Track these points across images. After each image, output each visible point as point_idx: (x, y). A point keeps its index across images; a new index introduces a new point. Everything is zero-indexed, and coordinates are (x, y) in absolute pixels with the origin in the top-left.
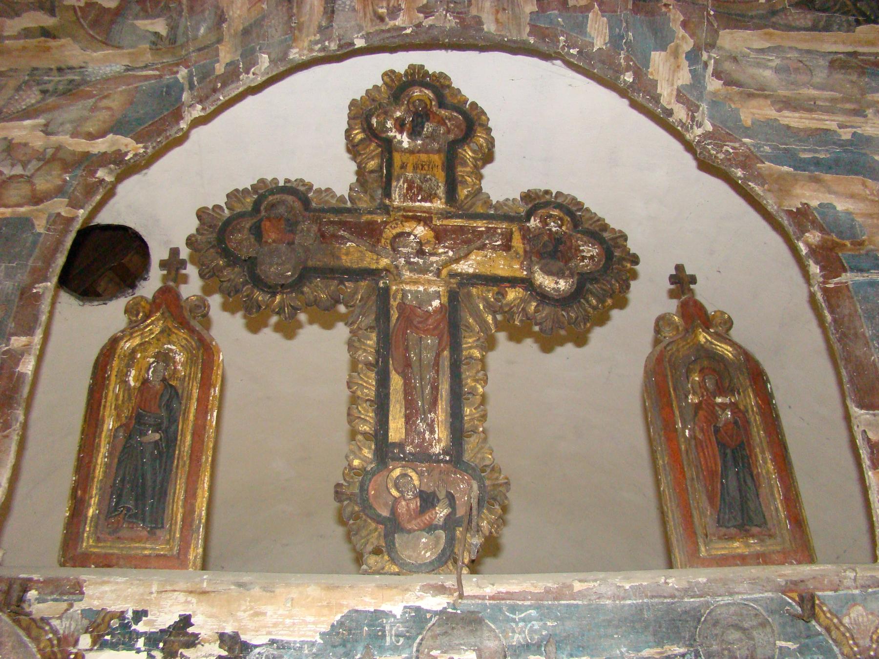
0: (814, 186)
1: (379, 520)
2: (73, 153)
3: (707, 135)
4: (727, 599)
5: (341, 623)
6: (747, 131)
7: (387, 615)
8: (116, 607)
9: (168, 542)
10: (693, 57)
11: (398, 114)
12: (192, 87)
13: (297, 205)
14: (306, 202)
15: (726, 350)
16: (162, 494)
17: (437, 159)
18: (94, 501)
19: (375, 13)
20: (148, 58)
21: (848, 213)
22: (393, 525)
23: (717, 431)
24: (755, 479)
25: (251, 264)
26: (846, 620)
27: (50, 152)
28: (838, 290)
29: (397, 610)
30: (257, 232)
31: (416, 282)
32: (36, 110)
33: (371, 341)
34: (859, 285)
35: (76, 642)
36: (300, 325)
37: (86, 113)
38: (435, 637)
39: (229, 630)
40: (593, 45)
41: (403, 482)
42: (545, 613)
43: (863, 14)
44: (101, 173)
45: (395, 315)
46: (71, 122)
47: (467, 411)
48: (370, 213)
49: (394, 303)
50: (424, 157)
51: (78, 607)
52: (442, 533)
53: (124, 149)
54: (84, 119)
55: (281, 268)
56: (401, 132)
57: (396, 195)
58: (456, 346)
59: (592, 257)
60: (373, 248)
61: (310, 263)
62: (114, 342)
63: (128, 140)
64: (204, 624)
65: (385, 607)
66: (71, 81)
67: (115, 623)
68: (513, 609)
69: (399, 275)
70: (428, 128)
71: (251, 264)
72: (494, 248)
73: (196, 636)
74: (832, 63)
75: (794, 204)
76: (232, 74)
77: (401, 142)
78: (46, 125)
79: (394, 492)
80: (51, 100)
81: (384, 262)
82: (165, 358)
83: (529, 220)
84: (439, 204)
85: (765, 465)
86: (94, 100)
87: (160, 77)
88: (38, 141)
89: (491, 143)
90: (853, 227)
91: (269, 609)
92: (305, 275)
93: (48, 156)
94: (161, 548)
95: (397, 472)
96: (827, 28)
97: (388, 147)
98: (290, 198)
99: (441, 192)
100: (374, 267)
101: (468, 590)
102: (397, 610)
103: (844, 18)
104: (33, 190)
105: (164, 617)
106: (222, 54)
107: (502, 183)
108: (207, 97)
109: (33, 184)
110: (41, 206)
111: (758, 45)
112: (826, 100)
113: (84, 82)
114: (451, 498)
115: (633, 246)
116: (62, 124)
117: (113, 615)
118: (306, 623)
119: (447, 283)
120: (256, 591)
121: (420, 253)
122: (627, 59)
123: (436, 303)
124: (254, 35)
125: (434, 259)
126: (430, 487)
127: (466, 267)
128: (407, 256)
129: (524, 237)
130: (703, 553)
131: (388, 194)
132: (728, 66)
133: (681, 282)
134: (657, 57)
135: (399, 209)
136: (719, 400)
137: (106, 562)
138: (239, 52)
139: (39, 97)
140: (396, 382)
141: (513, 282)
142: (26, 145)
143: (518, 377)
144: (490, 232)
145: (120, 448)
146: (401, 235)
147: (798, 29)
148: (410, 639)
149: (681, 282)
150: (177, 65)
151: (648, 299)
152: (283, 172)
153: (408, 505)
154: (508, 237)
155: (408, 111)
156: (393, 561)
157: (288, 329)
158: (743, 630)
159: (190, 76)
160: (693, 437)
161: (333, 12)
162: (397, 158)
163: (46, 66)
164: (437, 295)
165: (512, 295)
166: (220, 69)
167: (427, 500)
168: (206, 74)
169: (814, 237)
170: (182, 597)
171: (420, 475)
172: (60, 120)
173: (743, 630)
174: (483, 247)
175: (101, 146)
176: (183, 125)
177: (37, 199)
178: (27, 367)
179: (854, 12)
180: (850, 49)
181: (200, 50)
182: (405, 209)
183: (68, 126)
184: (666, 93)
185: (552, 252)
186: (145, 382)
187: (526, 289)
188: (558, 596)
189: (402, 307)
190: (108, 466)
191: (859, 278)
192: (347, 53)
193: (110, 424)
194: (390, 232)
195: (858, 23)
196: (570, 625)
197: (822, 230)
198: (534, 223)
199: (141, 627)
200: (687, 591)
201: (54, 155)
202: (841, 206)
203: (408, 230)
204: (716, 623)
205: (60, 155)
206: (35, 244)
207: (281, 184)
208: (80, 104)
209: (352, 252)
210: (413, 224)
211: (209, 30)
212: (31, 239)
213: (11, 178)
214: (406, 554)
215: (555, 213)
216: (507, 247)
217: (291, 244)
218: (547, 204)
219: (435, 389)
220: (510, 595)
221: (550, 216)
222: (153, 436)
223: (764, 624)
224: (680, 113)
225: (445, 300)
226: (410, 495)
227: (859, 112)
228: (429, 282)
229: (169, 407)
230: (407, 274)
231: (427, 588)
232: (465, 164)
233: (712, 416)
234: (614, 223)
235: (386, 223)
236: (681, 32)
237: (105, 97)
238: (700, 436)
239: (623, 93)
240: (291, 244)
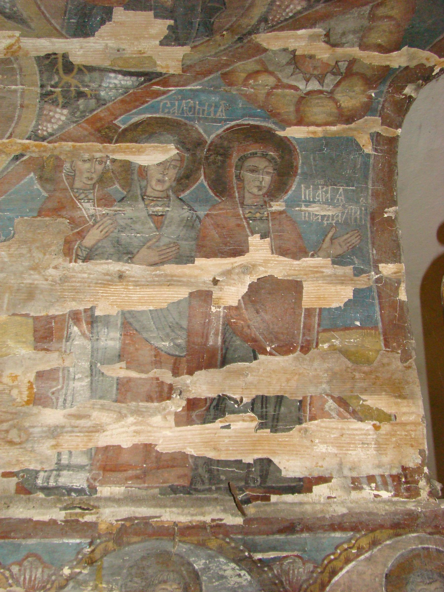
27: (343, 66)
32: (307, 18)
37: (365, 23)
53: (428, 65)
63: (426, 54)
86: (368, 8)
88: (323, 53)
93: (343, 70)
104: (339, 108)
109: (336, 102)
110: (353, 125)
116: (344, 34)
142: (312, 57)
175: (399, 59)
201: (349, 68)
205: (355, 69)
208: (355, 12)
213: (309, 93)
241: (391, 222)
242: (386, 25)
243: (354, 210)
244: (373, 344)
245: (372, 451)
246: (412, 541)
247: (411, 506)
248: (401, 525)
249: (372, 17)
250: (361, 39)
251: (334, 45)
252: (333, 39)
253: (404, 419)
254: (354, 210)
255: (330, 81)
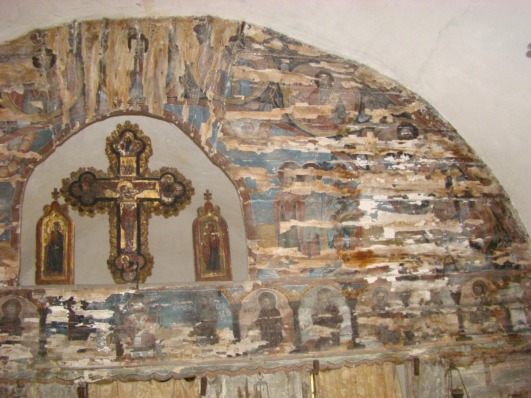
0: (246, 171)
1: (119, 270)
2: (19, 158)
3: (215, 155)
4: (204, 290)
5: (110, 297)
6: (228, 153)
7: (121, 295)
8: (54, 296)
9: (64, 276)
10: (215, 125)
11: (122, 143)
12: (55, 134)
13: (92, 177)
14: (94, 176)
15: (216, 218)
16: (61, 264)
17: (134, 159)
18: (43, 266)
19: (114, 102)
20: (38, 119)
21: (255, 180)
22: (123, 271)
23: (210, 243)
24: (218, 257)
25: (79, 198)
26: (232, 295)
27: (11, 157)
28: (247, 204)
29: (123, 294)
30: (81, 187)
31: (127, 201)
33: (115, 220)
34: (254, 203)
35: (45, 305)
36: (95, 214)
37: (20, 142)
38: (132, 300)
39: (83, 300)
40: (183, 119)
41: (125, 259)
42: (158, 294)
43: (276, 104)
44: (30, 166)
45: (122, 212)
46: (16, 145)
47: (142, 239)
48: (114, 179)
49: (121, 208)
50: (129, 158)
51: (45, 296)
52: (135, 272)
53: (36, 157)
54: (20, 144)
55: (88, 199)
56: (123, 150)
57: (121, 173)
58: (139, 222)
59: (179, 191)
60: (115, 191)
61: (97, 197)
62: (41, 219)
63: (36, 154)
64: (76, 298)
65: (120, 293)
66: (13, 128)
67: (55, 300)
68: (151, 293)
69: (123, 199)
70: (131, 147)
71: (79, 198)
72: (150, 189)
73: (75, 302)
74: (261, 125)
75: (237, 178)
76: (67, 130)
77: (122, 153)
78: (8, 146)
79: (123, 262)
80: (8, 136)
81: (118, 196)
82: (57, 224)
83: (161, 179)
84: (134, 175)
85: (222, 253)
86: (22, 136)
87: (43, 128)
88: (6, 153)
89: (151, 151)
90: (255, 185)
91: (92, 294)
92: (96, 201)
94: (63, 278)
95: (123, 257)
96: (262, 110)
97: (118, 155)
98: (89, 175)
99: (135, 171)
100: (115, 197)
101: (140, 288)
102: (123, 294)
103: (269, 105)
105: (67, 298)
106: (63, 120)
107: (154, 165)
108: (61, 139)
109: (8, 169)
111: (238, 118)
112: (256, 139)
113: (17, 129)
114: (138, 264)
115: (193, 185)
117: (54, 298)
118: (101, 297)
119: (136, 201)
120: (89, 290)
121: (129, 192)
122: (193, 127)
123: (133, 208)
124: (73, 112)
125: (132, 194)
126: (132, 260)
127: (142, 195)
128: (125, 193)
129: (160, 185)
130: (202, 276)
131: (119, 172)
132: (227, 126)
133: (208, 195)
134: (203, 125)
135: (122, 177)
136: (213, 234)
137: (48, 283)
138: (69, 119)
139: (3, 134)
140: (122, 231)
141: (156, 200)
143: (158, 226)
144: (149, 184)
145: (48, 251)
146: (123, 186)
147: (253, 110)
148: (126, 300)
149: (208, 195)
150: (49, 123)
151: (197, 201)
152: (86, 165)
153: (127, 265)
154: (155, 185)
155: (125, 141)
156: (123, 279)
157: (91, 212)
158: (207, 298)
159: (54, 129)
160: (203, 244)
161: (99, 102)
162: (122, 159)
163: (3, 121)
164: (134, 205)
165: (156, 203)
166: (63, 127)
167: (131, 264)
168: (59, 128)
169: (242, 189)
170: (71, 292)
171: (129, 257)
172: (13, 144)
173: (207, 298)
174: (147, 189)
175: (28, 155)
176: (54, 148)
177: (10, 175)
178: (18, 231)
179: (273, 103)
180: (268, 119)
181: (56, 117)
182: (124, 177)
183: (16, 147)
184: (203, 139)
185: (167, 189)
186: (52, 232)
187: (159, 202)
188: (162, 289)
189: (123, 209)
190: (45, 256)
191: (254, 201)
192: (104, 118)
193: (44, 245)
194: (120, 185)
195: (274, 107)
196: (165, 296)
197: (245, 186)
198: (163, 180)
199: (61, 300)
200: (194, 288)
201: (13, 158)
202: (252, 178)
203: (124, 184)
204: (200, 296)
205: (15, 158)
206: (13, 192)
207: (87, 170)
209: (109, 193)
210: (126, 182)
211: (58, 108)
212: (11, 190)
214: (126, 278)
215: (169, 176)
216: (154, 189)
217: (91, 190)
218: (167, 173)
219: (133, 233)
220: (150, 290)
221: (168, 177)
222: (57, 247)
223: (212, 296)
224: (207, 149)
225: (136, 206)
226: (127, 263)
227: (265, 144)
228: (132, 201)
229: (60, 239)
230: (125, 199)
231: (130, 288)
232: (142, 160)
233: (210, 239)
234: (188, 178)
235: (118, 183)
236: (212, 114)
237: (26, 135)
238: (205, 244)
239: (192, 138)
240: (91, 190)
241: (18, 210)
242: (26, 143)
243: (8, 205)
244: (8, 245)
245: (4, 275)
246: (10, 297)
247: (11, 288)
248: (7, 293)
249: (23, 140)
250: (18, 148)
251: (9, 150)
252: (10, 148)
253: (13, 266)
254: (8, 205)
255: (7, 162)
